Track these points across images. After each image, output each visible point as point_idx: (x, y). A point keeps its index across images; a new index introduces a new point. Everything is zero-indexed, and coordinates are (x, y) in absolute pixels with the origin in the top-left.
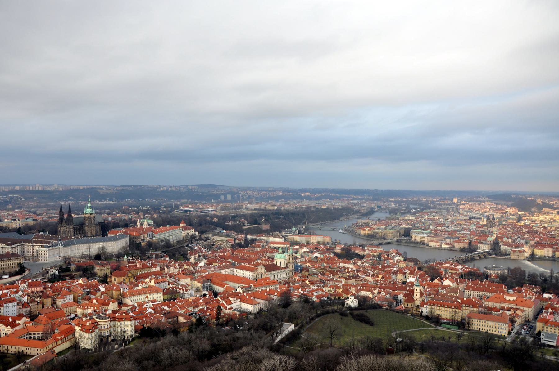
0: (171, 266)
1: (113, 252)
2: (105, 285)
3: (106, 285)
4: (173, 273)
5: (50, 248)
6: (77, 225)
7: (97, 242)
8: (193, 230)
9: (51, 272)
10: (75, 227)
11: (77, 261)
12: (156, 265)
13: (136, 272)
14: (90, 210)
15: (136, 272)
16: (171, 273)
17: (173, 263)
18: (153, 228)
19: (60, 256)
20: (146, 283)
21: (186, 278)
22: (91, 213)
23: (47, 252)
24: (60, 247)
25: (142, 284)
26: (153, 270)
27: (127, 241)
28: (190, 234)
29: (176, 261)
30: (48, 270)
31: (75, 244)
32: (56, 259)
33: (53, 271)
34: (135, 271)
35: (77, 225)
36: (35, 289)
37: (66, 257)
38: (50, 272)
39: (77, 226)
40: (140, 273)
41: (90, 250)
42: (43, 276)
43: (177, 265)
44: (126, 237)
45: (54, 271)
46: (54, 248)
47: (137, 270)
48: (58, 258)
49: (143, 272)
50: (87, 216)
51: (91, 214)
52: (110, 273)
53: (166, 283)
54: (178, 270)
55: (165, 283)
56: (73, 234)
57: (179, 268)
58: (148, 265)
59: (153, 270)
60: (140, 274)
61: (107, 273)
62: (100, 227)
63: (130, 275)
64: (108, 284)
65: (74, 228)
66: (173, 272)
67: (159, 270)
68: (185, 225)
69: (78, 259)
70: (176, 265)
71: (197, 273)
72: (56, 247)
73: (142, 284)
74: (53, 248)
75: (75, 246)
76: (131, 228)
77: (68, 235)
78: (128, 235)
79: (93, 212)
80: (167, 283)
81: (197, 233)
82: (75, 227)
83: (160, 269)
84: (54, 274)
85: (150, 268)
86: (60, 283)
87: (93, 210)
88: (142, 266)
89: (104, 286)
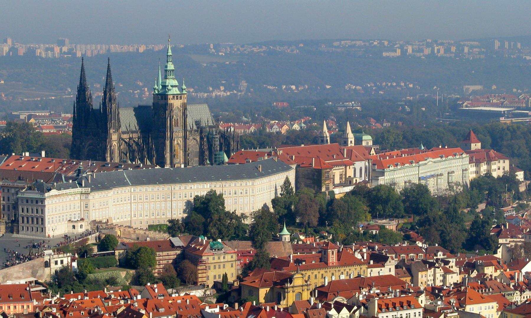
0: (432, 265)
1: (243, 216)
2: (221, 308)
3: (226, 306)
4: (441, 289)
5: (54, 192)
6: (133, 132)
7: (194, 181)
8: (507, 162)
9: (56, 263)
10: (125, 136)
11: (134, 236)
12: (385, 259)
13: (319, 276)
14: (175, 83)
15: (319, 276)
16: (433, 288)
17: (440, 256)
18: (373, 152)
19: (82, 219)
20: (349, 308)
21: (482, 300)
22: (176, 91)
23: (46, 202)
24: (84, 190)
25: (339, 311)
26: (375, 272)
27: (287, 182)
28: (495, 175)
29: (453, 253)
30: (46, 258)
31: (125, 184)
32: (71, 230)
33: (62, 262)
34: (316, 272)
35: (133, 132)
36: (12, 307)
37: (100, 222)
38: (53, 261)
39: (135, 136)
40: (333, 279)
41: (174, 205)
42: (33, 274)
43: (453, 262)
44: (289, 169)
45: (65, 263)
46: (64, 191)
47: (322, 271)
48: (78, 225)
49: (343, 277)
50: (162, 102)
51: (176, 97)
52: (234, 278)
53: (417, 311)
54: (454, 278)
55: (412, 312)
56: (117, 160)
57: (460, 273)
58: (358, 256)
59: (375, 272)
60: (330, 283)
61: (225, 277)
62: (202, 138)
63: (298, 281)
64: (232, 306)
65: (123, 140)
66: (439, 283)
67: (393, 273)
68: (479, 146)
69: (137, 232)
70: (449, 262)
71: (522, 291)
72: (71, 190)
73: (339, 311)
74: (61, 192)
75: (128, 188)
76: (303, 146)
77: (104, 159)
78: (294, 166)
79: (181, 90)
80: (421, 310)
81: (520, 175)
82: (125, 136)
83: (397, 273)
84: (64, 270)
85: (364, 267)
86: (86, 295)
87: (180, 83)
88: (339, 259)
89: (217, 310)
